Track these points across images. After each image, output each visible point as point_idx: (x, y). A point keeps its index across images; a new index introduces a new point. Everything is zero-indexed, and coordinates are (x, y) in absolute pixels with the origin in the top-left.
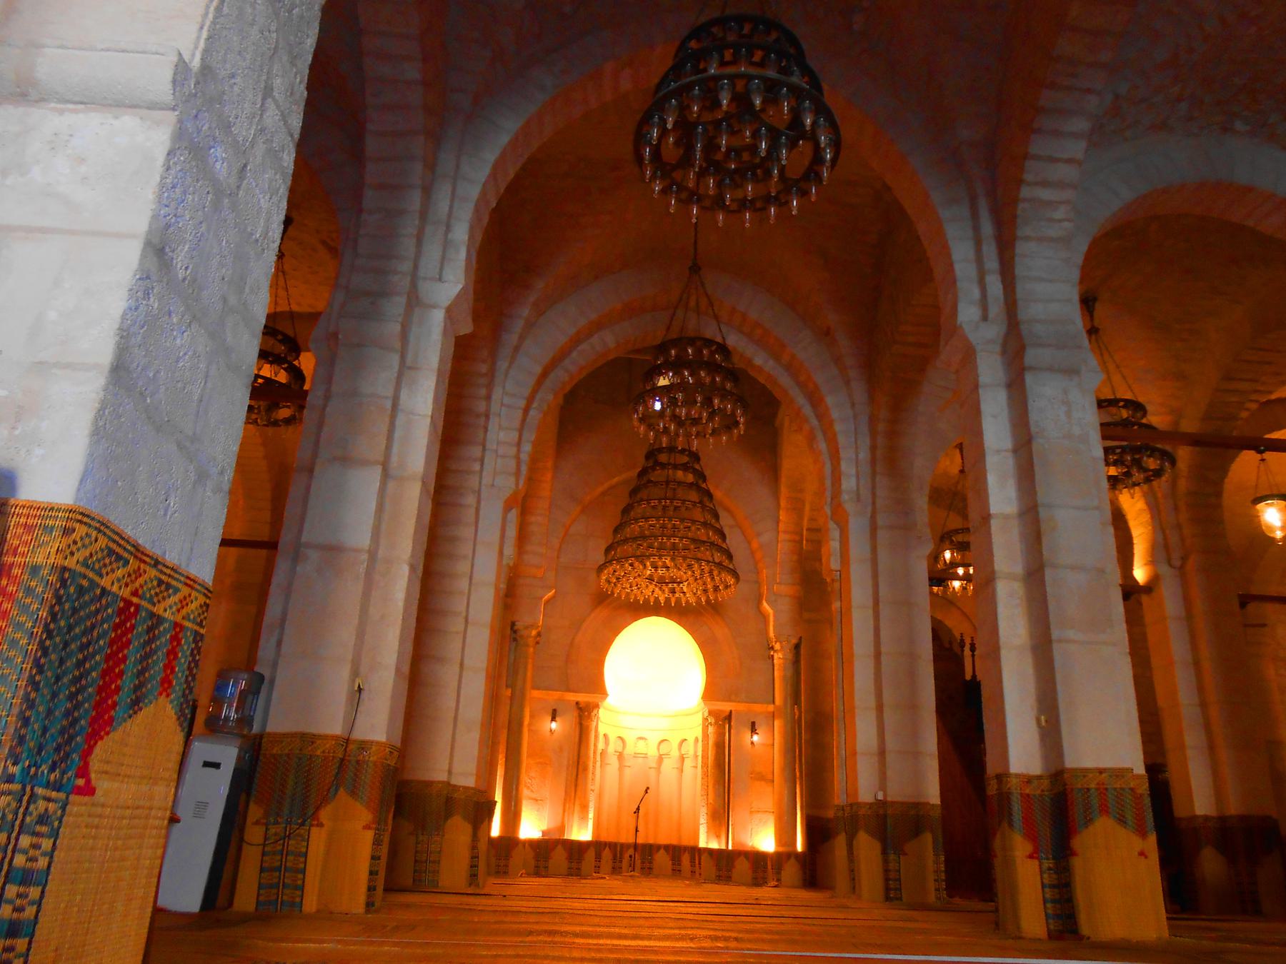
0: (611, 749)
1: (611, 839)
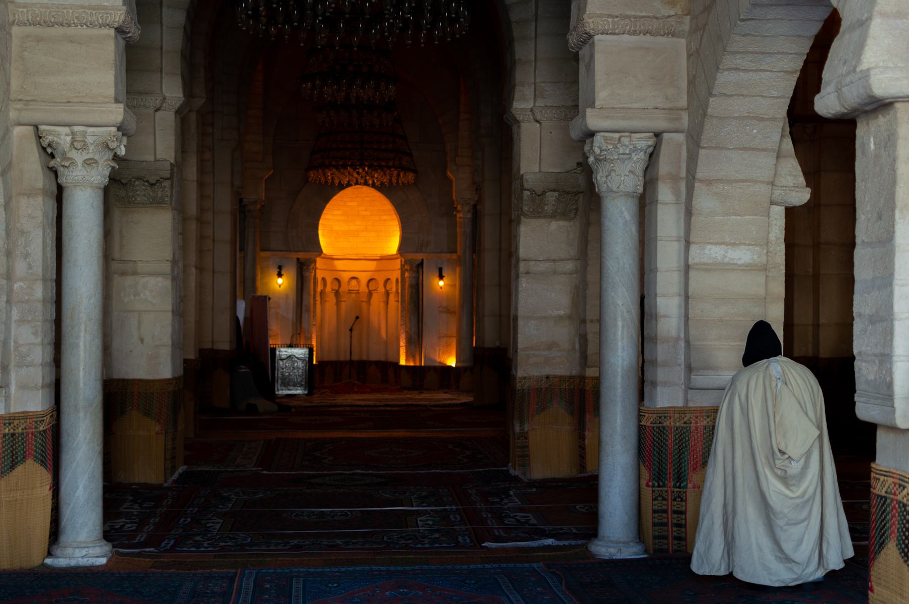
0: (328, 289)
1: (333, 358)
